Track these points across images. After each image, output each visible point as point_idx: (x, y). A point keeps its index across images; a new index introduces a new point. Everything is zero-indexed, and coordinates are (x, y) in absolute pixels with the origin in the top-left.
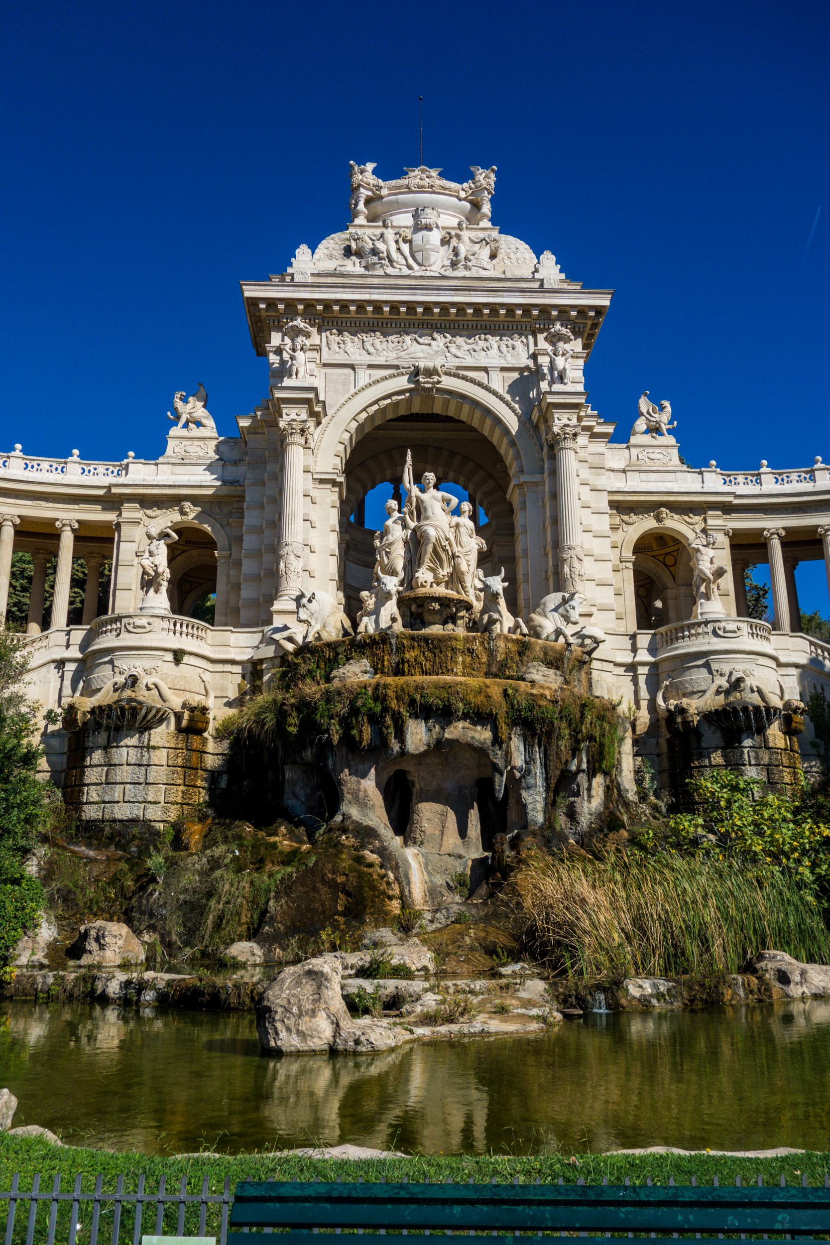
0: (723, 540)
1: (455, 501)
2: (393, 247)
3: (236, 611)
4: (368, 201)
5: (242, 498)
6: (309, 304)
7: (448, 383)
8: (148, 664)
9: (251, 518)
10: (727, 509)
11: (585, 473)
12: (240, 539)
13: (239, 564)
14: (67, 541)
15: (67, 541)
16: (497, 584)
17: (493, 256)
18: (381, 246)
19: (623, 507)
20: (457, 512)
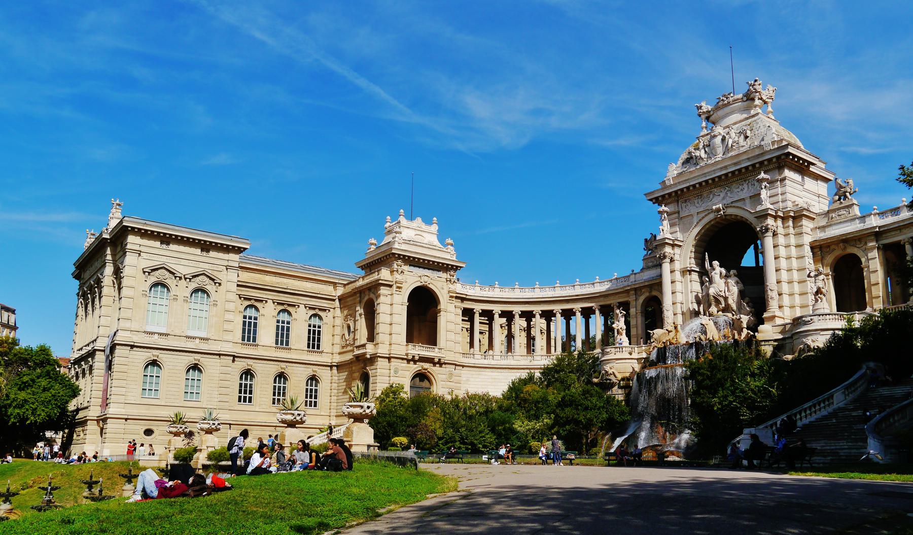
0: (875, 253)
2: (703, 151)
7: (730, 211)
10: (878, 234)
17: (746, 137)
19: (819, 249)
20: (727, 277)
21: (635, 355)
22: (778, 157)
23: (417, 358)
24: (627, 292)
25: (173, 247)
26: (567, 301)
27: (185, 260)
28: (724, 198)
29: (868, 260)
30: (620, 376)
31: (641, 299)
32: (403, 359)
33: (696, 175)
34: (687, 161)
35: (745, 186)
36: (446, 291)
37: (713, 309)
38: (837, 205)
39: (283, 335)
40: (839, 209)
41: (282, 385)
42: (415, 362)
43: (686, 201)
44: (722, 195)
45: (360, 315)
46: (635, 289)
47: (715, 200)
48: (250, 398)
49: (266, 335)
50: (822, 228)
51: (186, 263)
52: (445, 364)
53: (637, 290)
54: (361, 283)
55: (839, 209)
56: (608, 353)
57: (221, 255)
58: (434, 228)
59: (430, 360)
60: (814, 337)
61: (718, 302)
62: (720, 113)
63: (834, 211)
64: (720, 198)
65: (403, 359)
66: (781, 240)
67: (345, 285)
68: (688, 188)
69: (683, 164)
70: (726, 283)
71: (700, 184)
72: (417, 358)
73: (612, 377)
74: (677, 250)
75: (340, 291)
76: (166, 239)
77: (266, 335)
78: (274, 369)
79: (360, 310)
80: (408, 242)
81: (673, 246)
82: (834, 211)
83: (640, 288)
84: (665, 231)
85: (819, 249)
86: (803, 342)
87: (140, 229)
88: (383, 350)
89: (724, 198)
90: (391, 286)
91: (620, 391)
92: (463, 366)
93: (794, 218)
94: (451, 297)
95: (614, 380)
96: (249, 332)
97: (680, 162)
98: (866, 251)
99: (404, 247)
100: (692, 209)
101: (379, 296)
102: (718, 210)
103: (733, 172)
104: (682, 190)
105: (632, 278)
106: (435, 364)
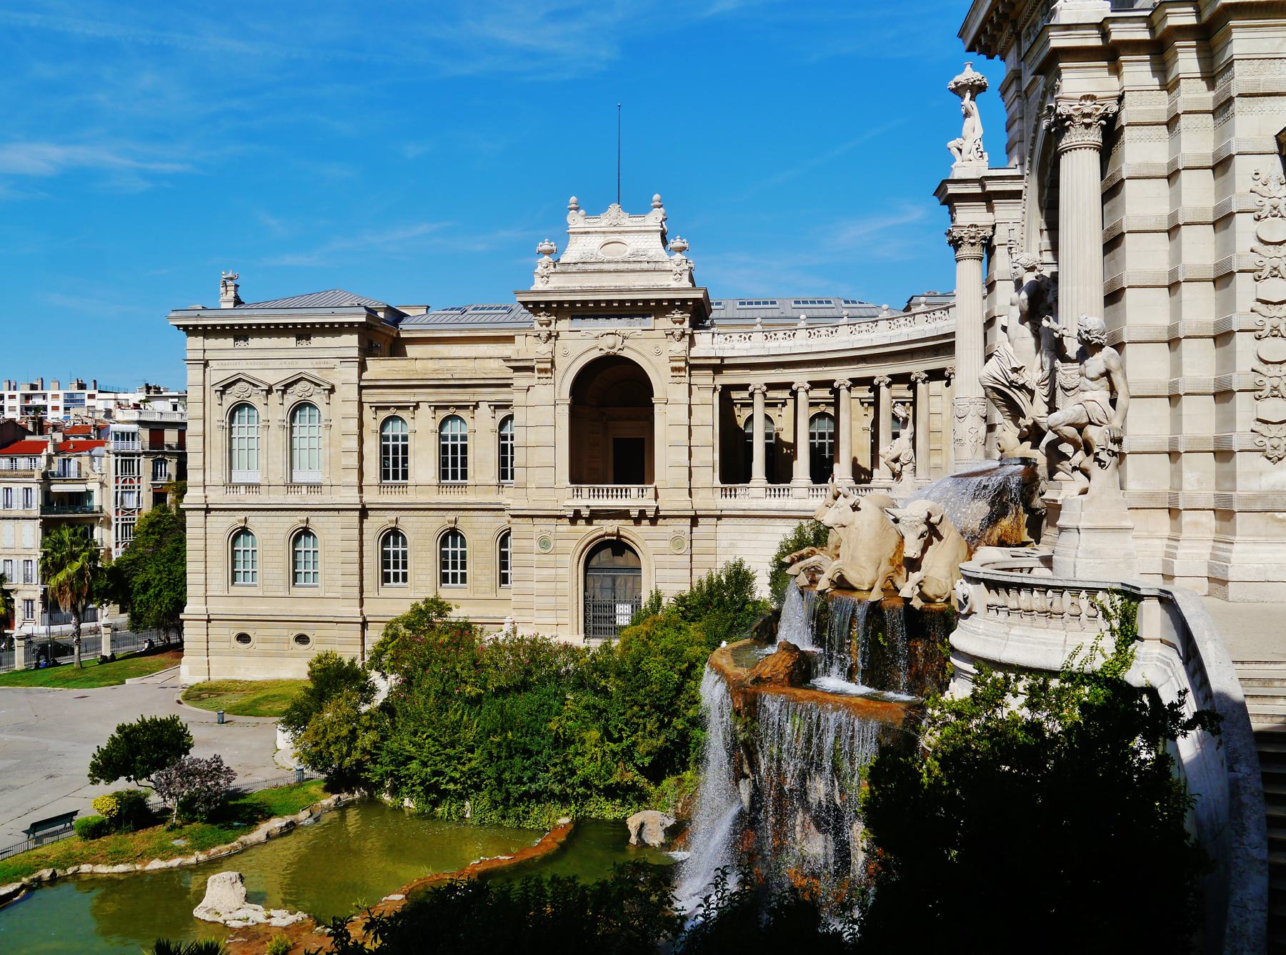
23: (586, 513)
25: (254, 342)
27: (270, 360)
32: (559, 517)
36: (665, 358)
39: (453, 462)
41: (459, 549)
42: (589, 521)
48: (405, 575)
49: (423, 464)
51: (276, 364)
52: (665, 517)
57: (329, 341)
58: (654, 219)
59: (623, 514)
65: (559, 517)
66: (1140, 151)
72: (586, 513)
74: (1005, 212)
76: (241, 333)
77: (423, 464)
78: (439, 523)
80: (583, 268)
81: (988, 199)
87: (196, 326)
90: (531, 369)
92: (719, 518)
94: (674, 369)
96: (394, 463)
99: (556, 282)
106: (637, 521)
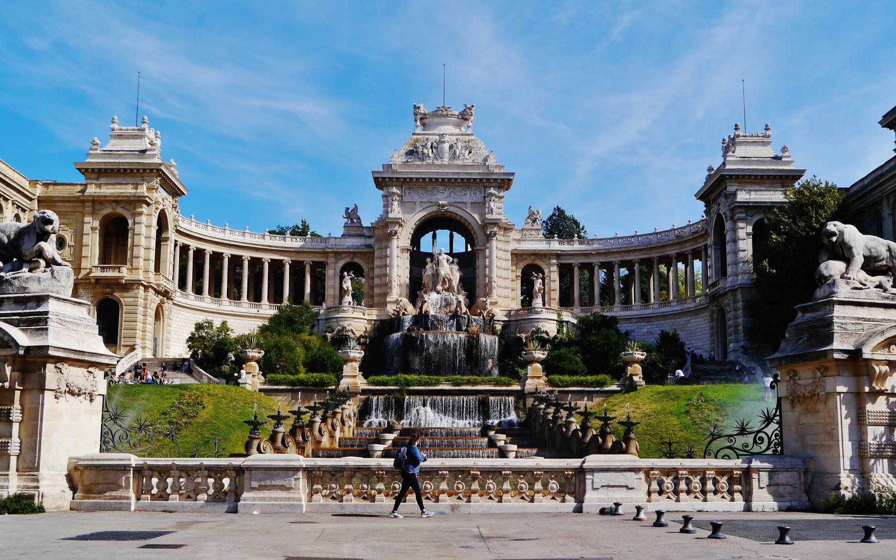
1: (451, 259)
3: (372, 297)
4: (421, 119)
5: (373, 253)
6: (397, 179)
7: (452, 209)
8: (348, 322)
9: (377, 263)
10: (558, 255)
11: (501, 245)
12: (373, 269)
13: (373, 278)
14: (308, 268)
15: (308, 268)
16: (461, 298)
17: (470, 152)
18: (426, 151)
19: (517, 256)
21: (366, 317)
22: (502, 180)
24: (325, 253)
26: (257, 250)
28: (447, 197)
29: (550, 272)
30: (358, 334)
31: (341, 263)
33: (419, 170)
34: (410, 153)
35: (468, 192)
37: (439, 287)
38: (529, 226)
40: (531, 230)
43: (410, 188)
44: (446, 194)
45: (93, 229)
46: (335, 253)
47: (439, 196)
50: (519, 241)
53: (338, 254)
54: (92, 190)
55: (531, 230)
56: (344, 311)
60: (543, 324)
61: (444, 282)
62: (437, 120)
63: (528, 230)
64: (444, 196)
67: (46, 185)
68: (417, 179)
69: (406, 154)
70: (451, 270)
71: (430, 179)
73: (350, 334)
75: (39, 191)
79: (92, 224)
82: (528, 230)
83: (341, 253)
84: (396, 211)
85: (517, 256)
86: (534, 326)
88: (141, 276)
89: (447, 197)
91: (358, 347)
93: (505, 229)
95: (352, 336)
97: (403, 152)
98: (549, 265)
100: (413, 196)
101: (141, 214)
102: (443, 206)
103: (462, 179)
104: (411, 179)
105: (332, 242)
